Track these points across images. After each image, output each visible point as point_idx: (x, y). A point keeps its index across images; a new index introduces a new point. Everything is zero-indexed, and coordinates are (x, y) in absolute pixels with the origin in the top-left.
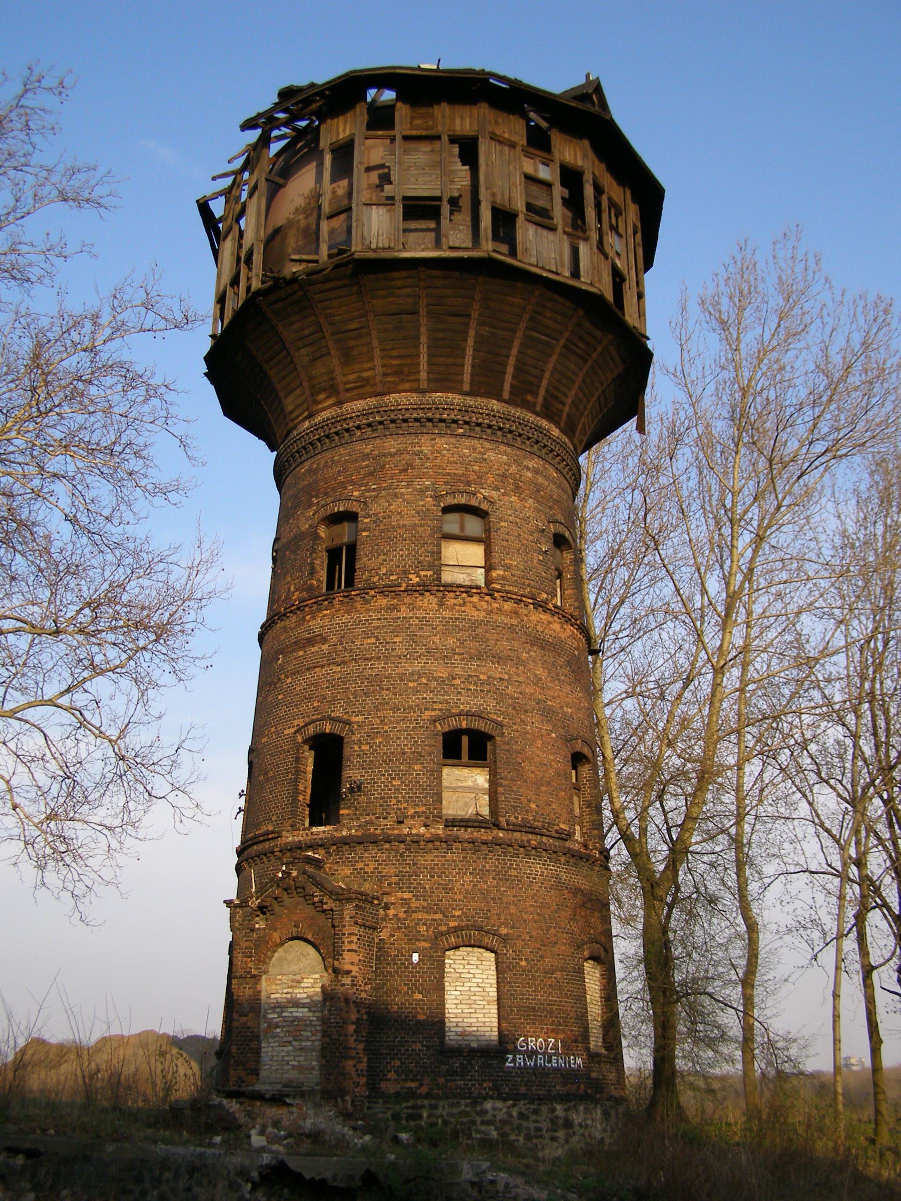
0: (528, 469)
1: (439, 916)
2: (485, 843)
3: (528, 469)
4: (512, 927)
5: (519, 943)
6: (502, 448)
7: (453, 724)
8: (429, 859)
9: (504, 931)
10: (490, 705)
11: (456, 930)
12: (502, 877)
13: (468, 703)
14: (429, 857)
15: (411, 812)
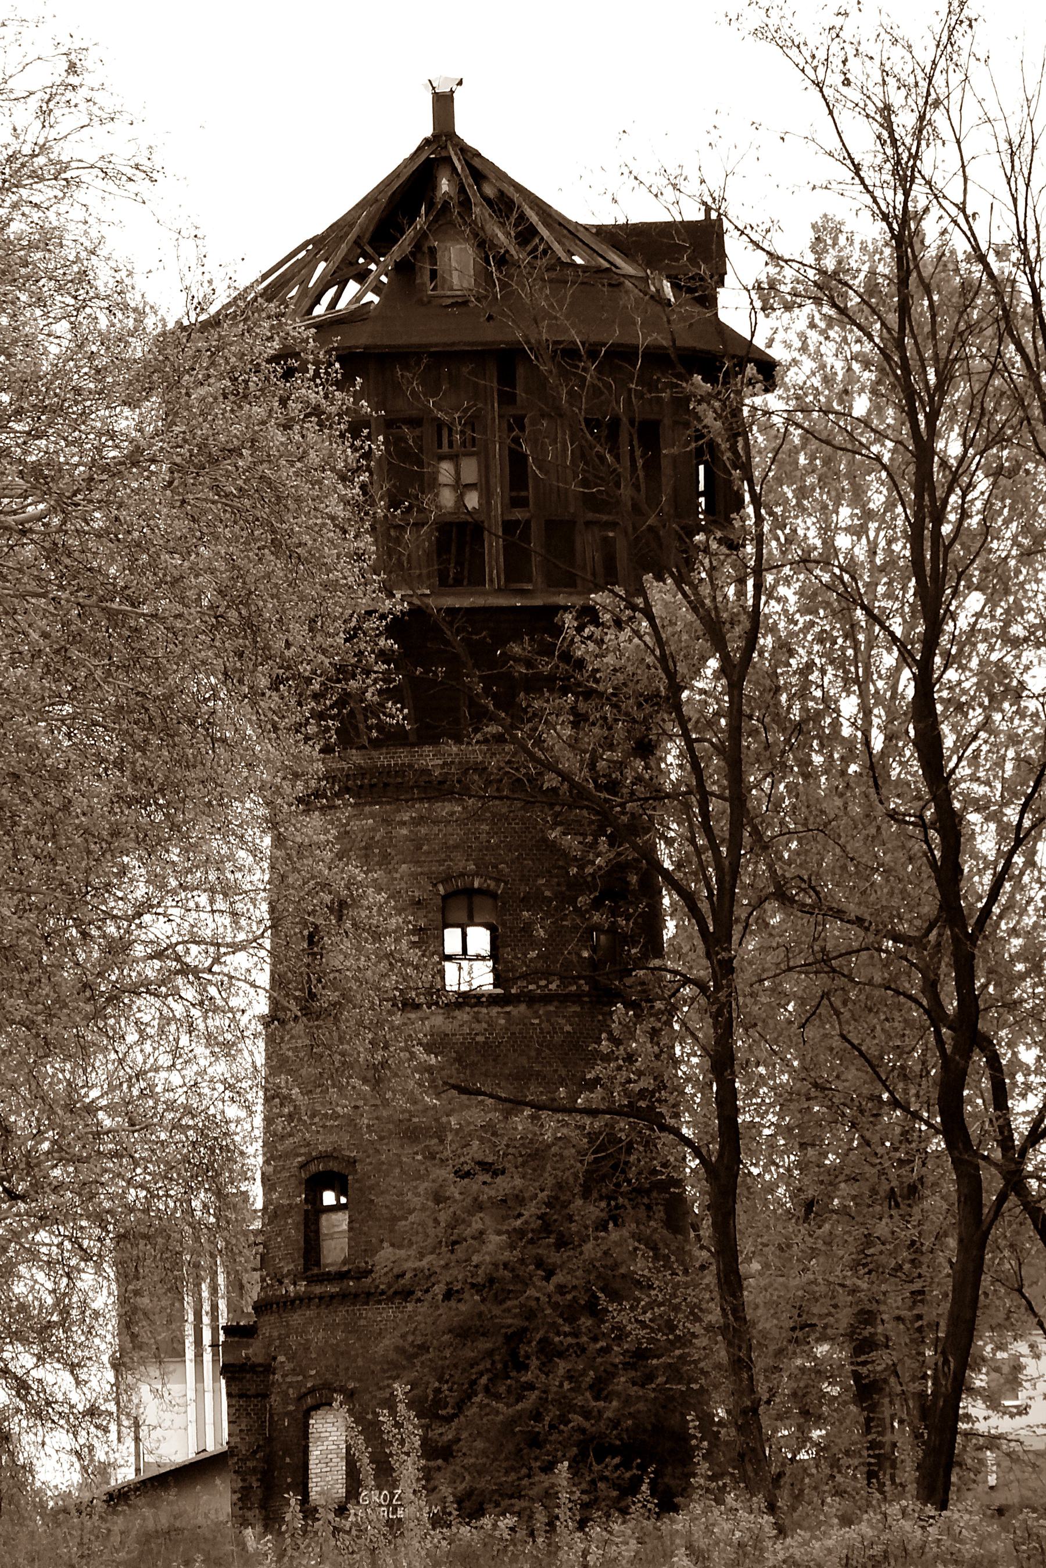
0: (403, 823)
1: (300, 1378)
2: (332, 1297)
3: (403, 823)
4: (360, 1380)
5: (367, 1397)
6: (367, 809)
7: (313, 1168)
8: (296, 1319)
9: (351, 1385)
10: (342, 1140)
11: (312, 1391)
12: (352, 1328)
13: (324, 1143)
14: (295, 1317)
15: (285, 1270)
